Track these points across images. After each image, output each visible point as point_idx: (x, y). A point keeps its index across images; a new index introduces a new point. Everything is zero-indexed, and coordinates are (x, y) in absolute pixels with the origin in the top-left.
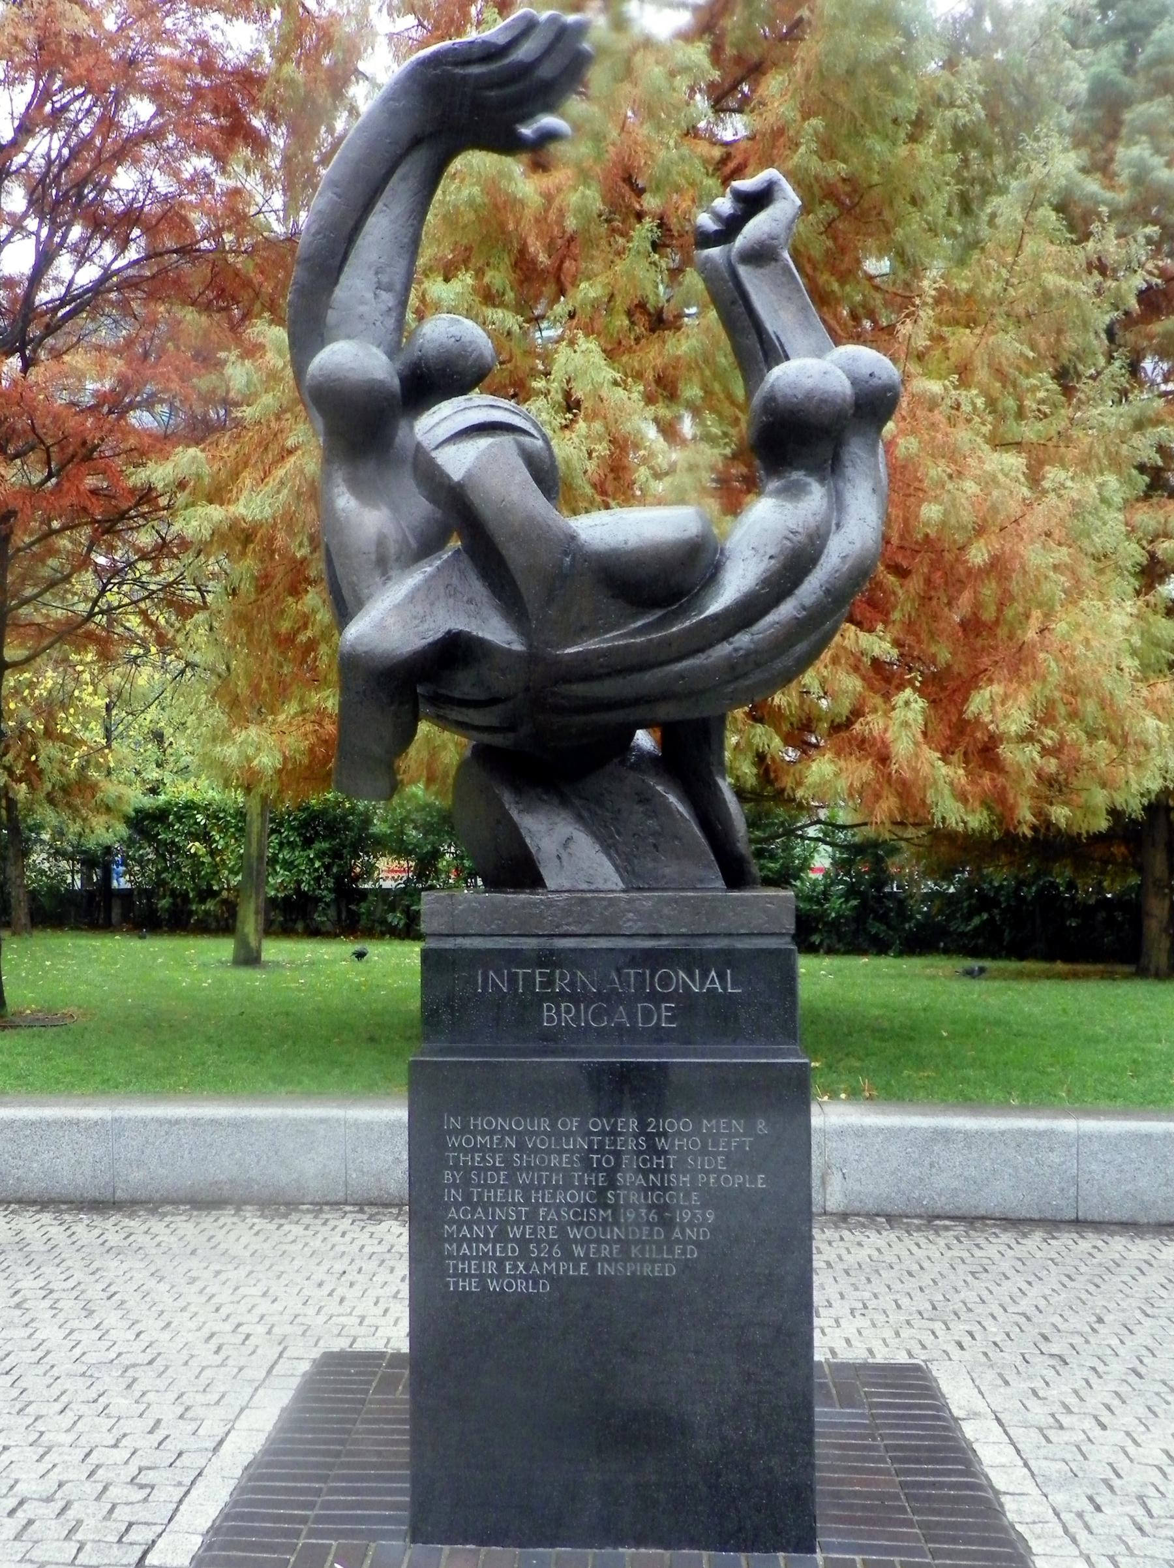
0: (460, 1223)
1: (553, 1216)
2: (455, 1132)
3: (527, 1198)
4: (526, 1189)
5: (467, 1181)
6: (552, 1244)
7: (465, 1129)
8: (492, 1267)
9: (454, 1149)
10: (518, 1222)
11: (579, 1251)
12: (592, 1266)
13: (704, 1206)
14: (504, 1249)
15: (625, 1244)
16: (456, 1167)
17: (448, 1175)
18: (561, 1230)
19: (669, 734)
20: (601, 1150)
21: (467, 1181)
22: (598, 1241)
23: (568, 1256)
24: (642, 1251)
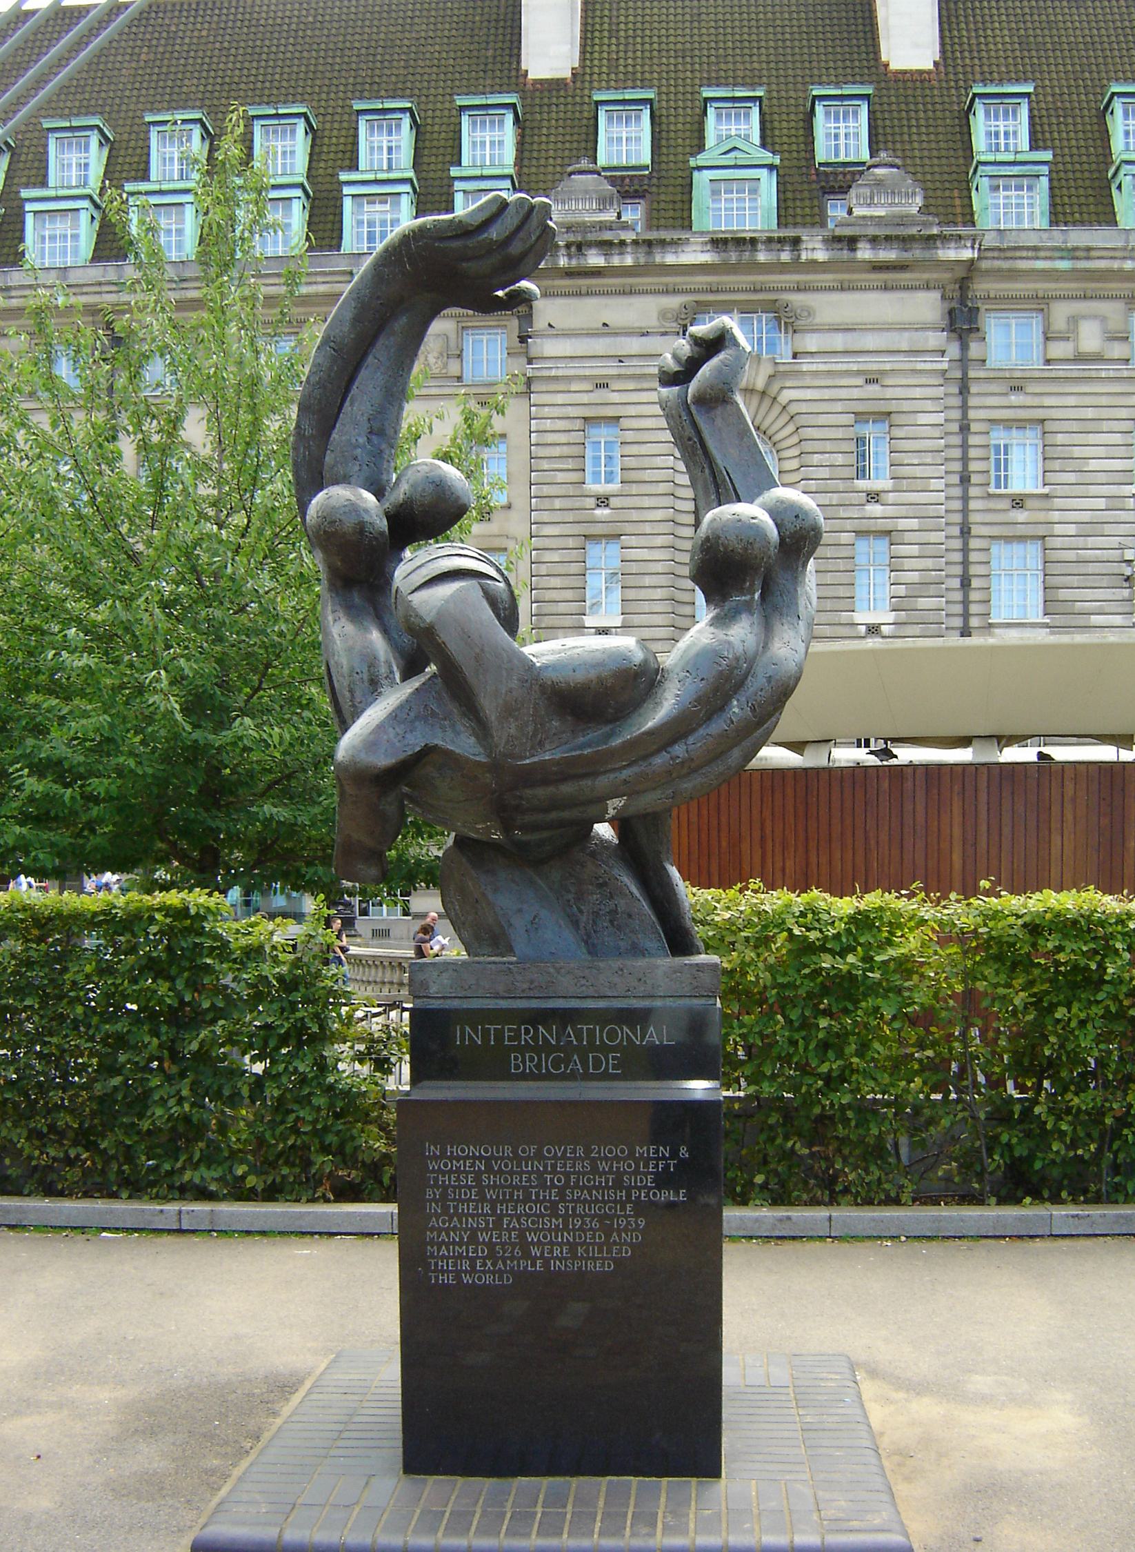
0: (440, 1230)
1: (515, 1223)
2: (435, 1158)
3: (493, 1209)
4: (493, 1204)
5: (444, 1196)
6: (514, 1245)
7: (443, 1154)
8: (466, 1265)
9: (433, 1171)
10: (487, 1229)
11: (535, 1251)
12: (546, 1263)
13: (637, 1215)
14: (476, 1251)
15: (573, 1247)
16: (436, 1185)
17: (429, 1192)
18: (522, 1235)
19: (623, 824)
20: (554, 1172)
21: (444, 1196)
22: (551, 1243)
23: (526, 1255)
24: (587, 1251)
